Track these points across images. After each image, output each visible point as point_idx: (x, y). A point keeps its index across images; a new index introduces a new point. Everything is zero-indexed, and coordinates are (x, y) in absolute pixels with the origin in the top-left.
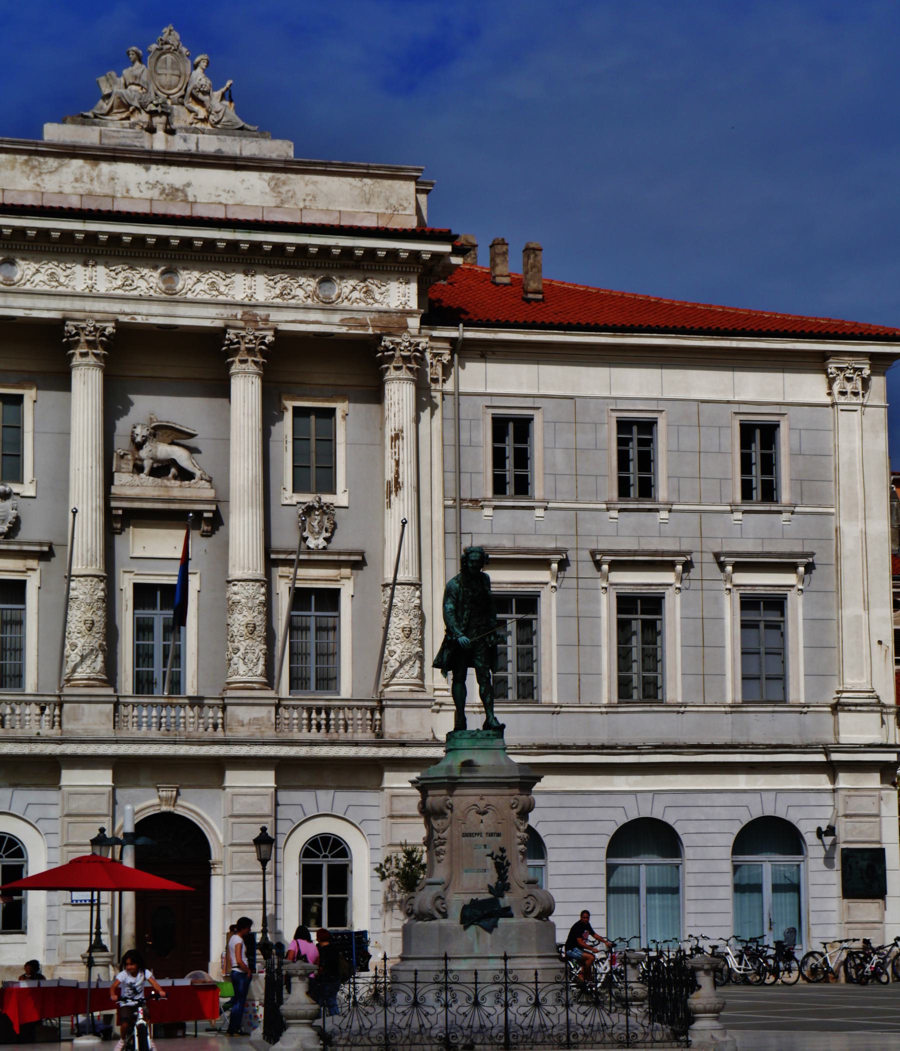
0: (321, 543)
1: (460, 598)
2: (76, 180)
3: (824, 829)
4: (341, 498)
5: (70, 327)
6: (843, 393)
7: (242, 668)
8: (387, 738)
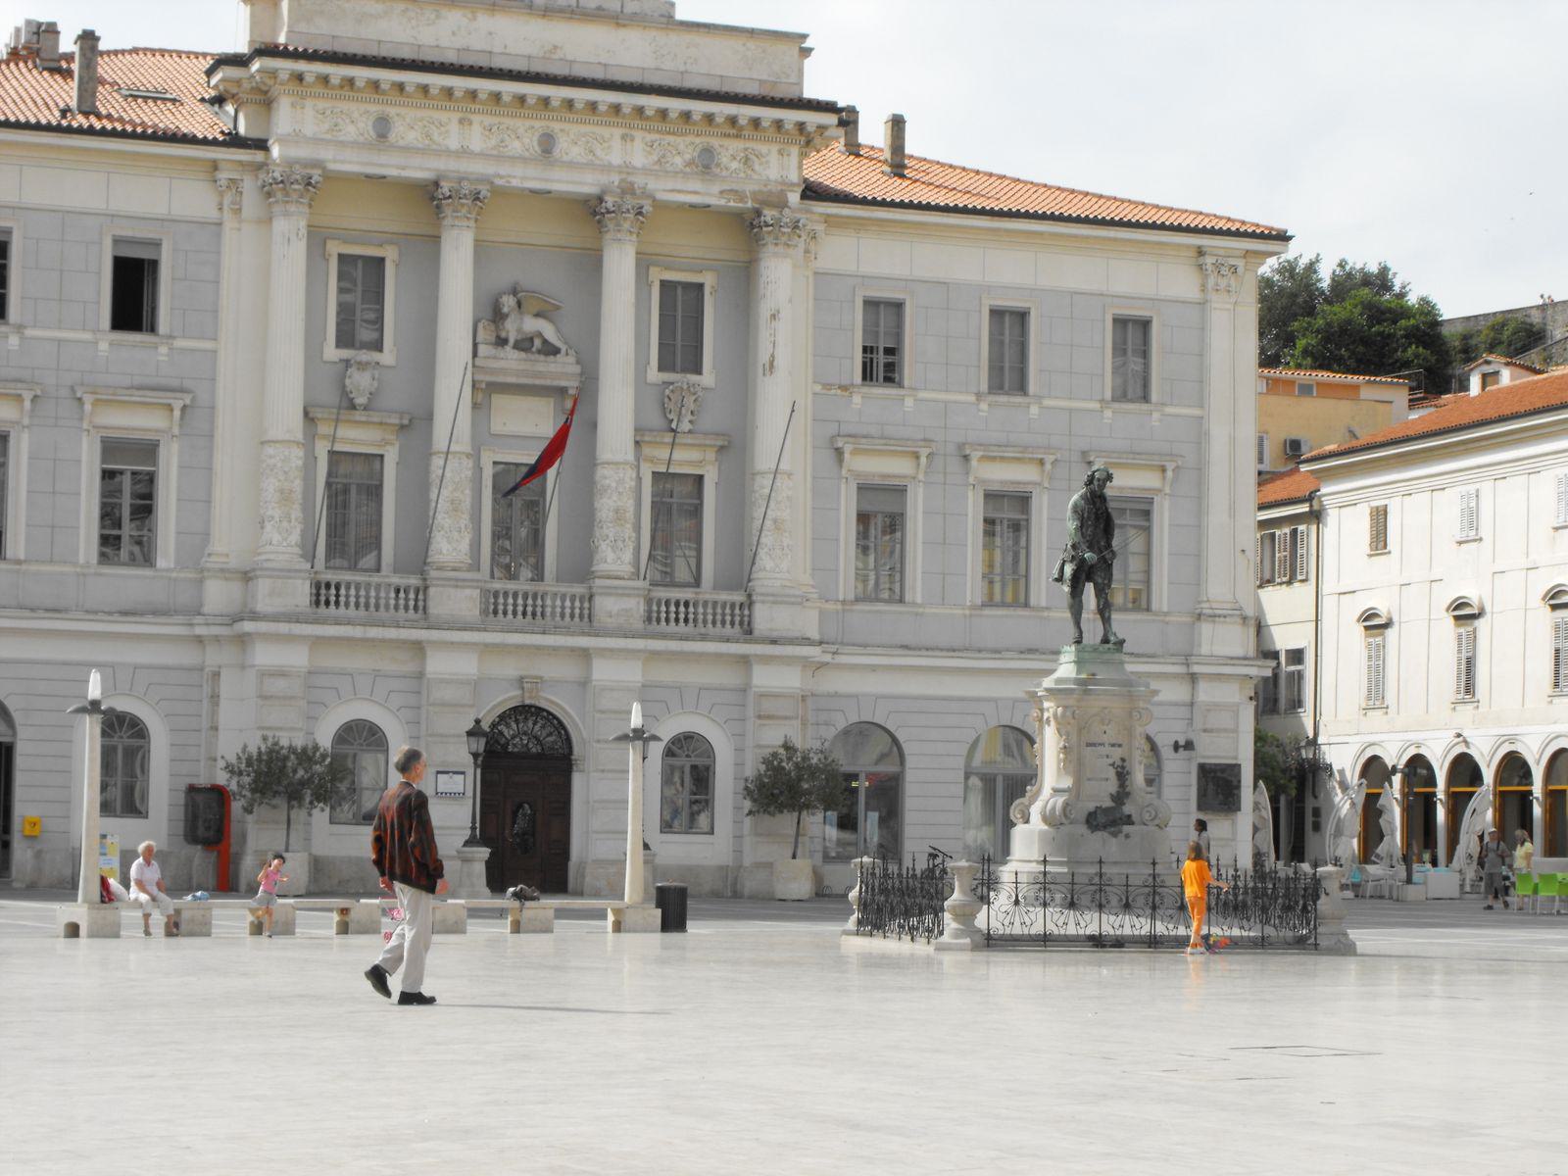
2: (454, 34)
3: (1182, 742)
4: (708, 378)
5: (446, 187)
7: (610, 556)
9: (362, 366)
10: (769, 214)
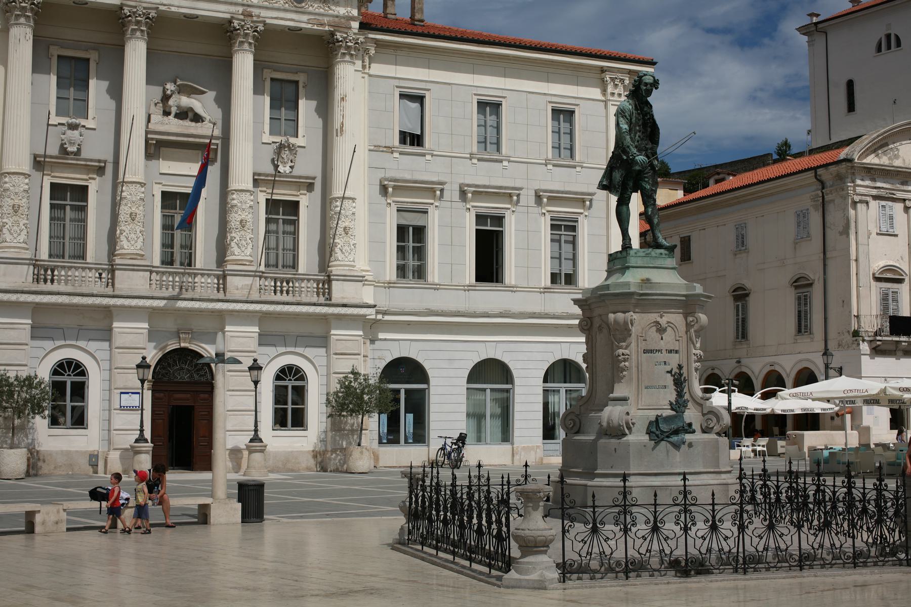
0: (288, 169)
1: (634, 120)
4: (299, 141)
5: (126, 11)
6: (613, 94)
8: (334, 301)
9: (73, 127)
10: (339, 36)
